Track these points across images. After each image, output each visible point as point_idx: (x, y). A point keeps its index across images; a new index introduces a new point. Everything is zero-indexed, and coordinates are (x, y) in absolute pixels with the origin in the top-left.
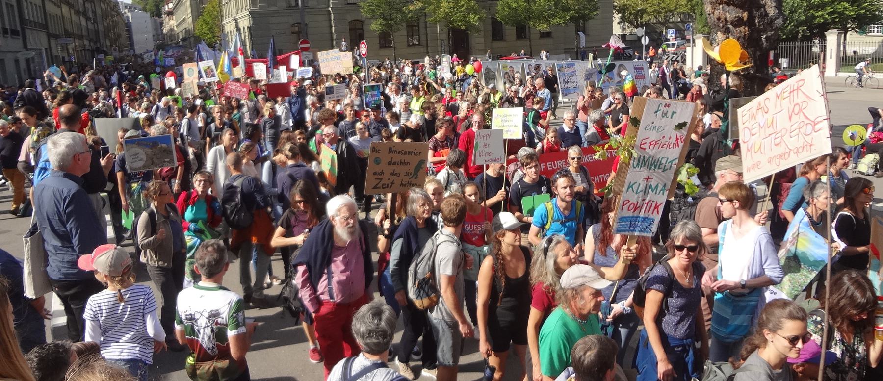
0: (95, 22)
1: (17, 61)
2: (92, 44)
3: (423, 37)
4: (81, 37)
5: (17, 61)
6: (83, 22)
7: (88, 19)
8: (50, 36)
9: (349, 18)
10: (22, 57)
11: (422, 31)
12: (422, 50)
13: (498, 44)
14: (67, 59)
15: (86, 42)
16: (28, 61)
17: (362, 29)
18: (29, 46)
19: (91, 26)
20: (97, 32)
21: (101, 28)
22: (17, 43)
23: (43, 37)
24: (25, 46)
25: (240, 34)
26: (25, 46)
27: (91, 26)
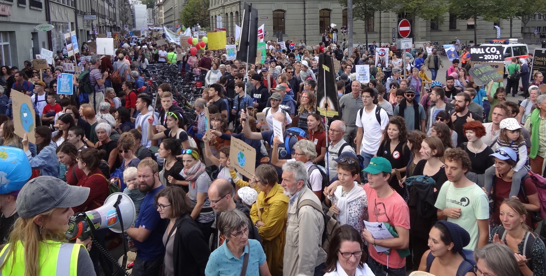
0: (114, 7)
1: (35, 34)
2: (111, 22)
3: (377, 26)
4: (104, 17)
5: (35, 34)
6: (106, 6)
7: (110, 4)
8: (76, 12)
9: (321, 6)
11: (376, 20)
13: (435, 34)
14: (91, 33)
15: (107, 21)
16: (49, 33)
17: (329, 17)
18: (52, 19)
19: (111, 10)
20: (115, 15)
21: (118, 12)
22: (39, 16)
23: (71, 14)
24: (48, 19)
25: (238, 16)
26: (48, 19)
27: (111, 10)
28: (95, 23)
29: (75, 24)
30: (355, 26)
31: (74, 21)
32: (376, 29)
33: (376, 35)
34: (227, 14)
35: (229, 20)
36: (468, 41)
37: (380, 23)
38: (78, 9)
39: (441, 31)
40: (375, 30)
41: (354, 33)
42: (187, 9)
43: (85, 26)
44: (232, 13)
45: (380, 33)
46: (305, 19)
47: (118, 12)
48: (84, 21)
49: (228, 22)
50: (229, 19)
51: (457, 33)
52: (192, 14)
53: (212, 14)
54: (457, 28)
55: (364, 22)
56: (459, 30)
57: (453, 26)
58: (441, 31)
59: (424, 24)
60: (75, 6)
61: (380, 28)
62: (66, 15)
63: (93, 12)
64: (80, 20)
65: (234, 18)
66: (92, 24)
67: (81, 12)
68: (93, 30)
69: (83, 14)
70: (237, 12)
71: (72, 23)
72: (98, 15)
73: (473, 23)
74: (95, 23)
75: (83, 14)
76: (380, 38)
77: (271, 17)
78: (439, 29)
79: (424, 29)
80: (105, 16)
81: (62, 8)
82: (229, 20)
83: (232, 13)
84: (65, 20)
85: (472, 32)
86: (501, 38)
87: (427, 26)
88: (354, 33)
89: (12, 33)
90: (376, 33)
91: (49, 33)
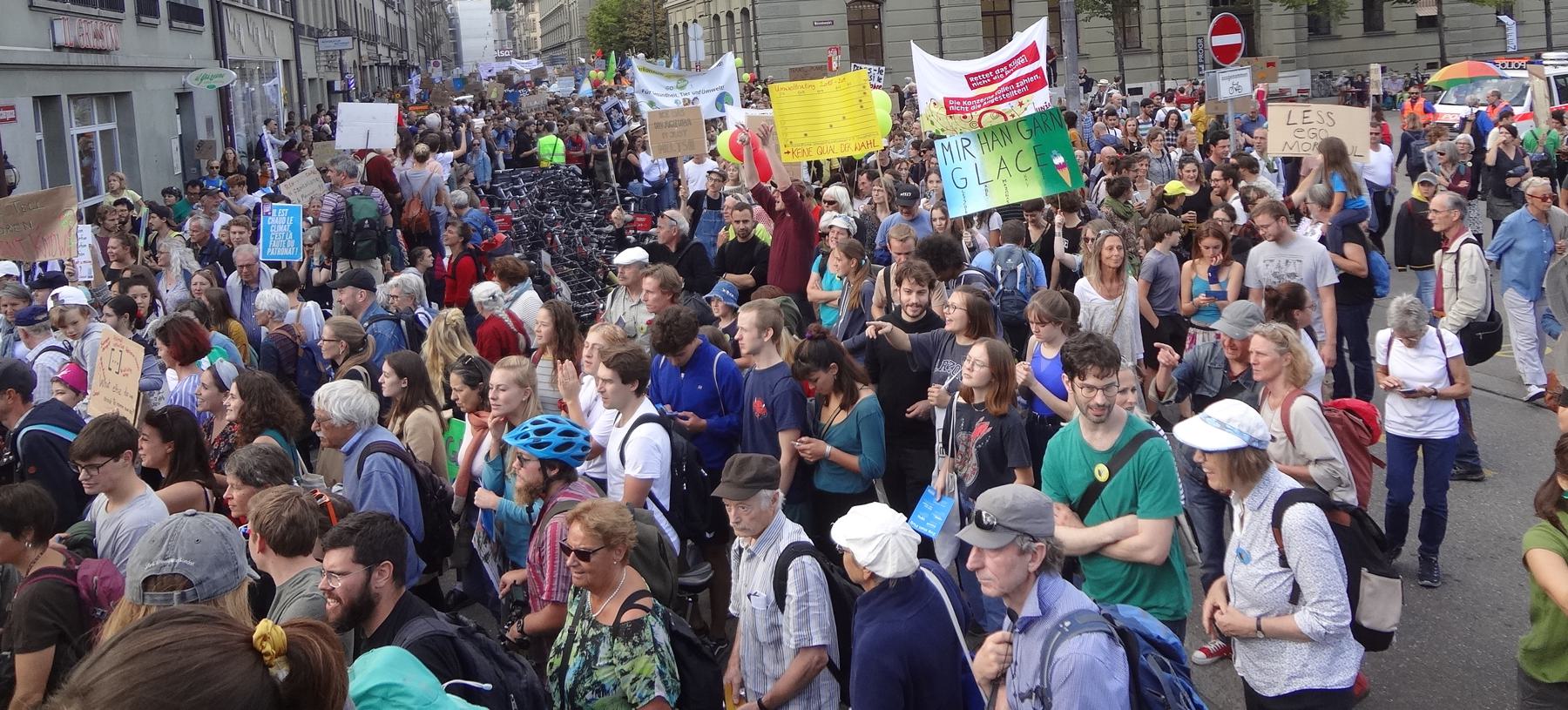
0: (401, 12)
2: (393, 54)
4: (372, 40)
5: (184, 98)
6: (379, 9)
8: (297, 30)
10: (206, 81)
12: (1152, 61)
14: (338, 87)
15: (383, 51)
16: (224, 94)
17: (1010, 13)
18: (232, 52)
20: (403, 31)
21: (411, 24)
23: (282, 36)
24: (220, 53)
26: (220, 53)
28: (349, 58)
29: (293, 65)
30: (1084, 35)
31: (290, 55)
32: (1149, 41)
33: (1148, 58)
34: (717, 18)
35: (724, 35)
36: (1422, 65)
37: (1160, 23)
38: (302, 21)
39: (1338, 38)
40: (1144, 46)
41: (1086, 57)
42: (603, 9)
43: (322, 69)
44: (730, 15)
45: (1161, 52)
46: (940, 23)
47: (411, 24)
48: (317, 53)
49: (720, 40)
50: (724, 30)
51: (1389, 42)
52: (619, 21)
53: (676, 18)
54: (1387, 28)
55: (1111, 22)
56: (1392, 34)
57: (1373, 24)
58: (1338, 38)
59: (1289, 21)
60: (294, 13)
61: (1160, 38)
62: (270, 40)
63: (343, 29)
64: (307, 51)
65: (738, 27)
66: (341, 61)
67: (311, 29)
68: (343, 78)
69: (317, 35)
70: (745, 12)
71: (286, 62)
72: (358, 36)
73: (1433, 11)
74: (349, 58)
75: (317, 35)
76: (1162, 66)
77: (842, 21)
78: (1337, 30)
79: (1290, 36)
80: (376, 37)
81: (258, 20)
82: (724, 35)
83: (730, 15)
84: (268, 54)
85: (1432, 38)
86: (1519, 51)
87: (1297, 27)
88: (1086, 57)
89: (123, 97)
90: (1149, 52)
91: (224, 94)
